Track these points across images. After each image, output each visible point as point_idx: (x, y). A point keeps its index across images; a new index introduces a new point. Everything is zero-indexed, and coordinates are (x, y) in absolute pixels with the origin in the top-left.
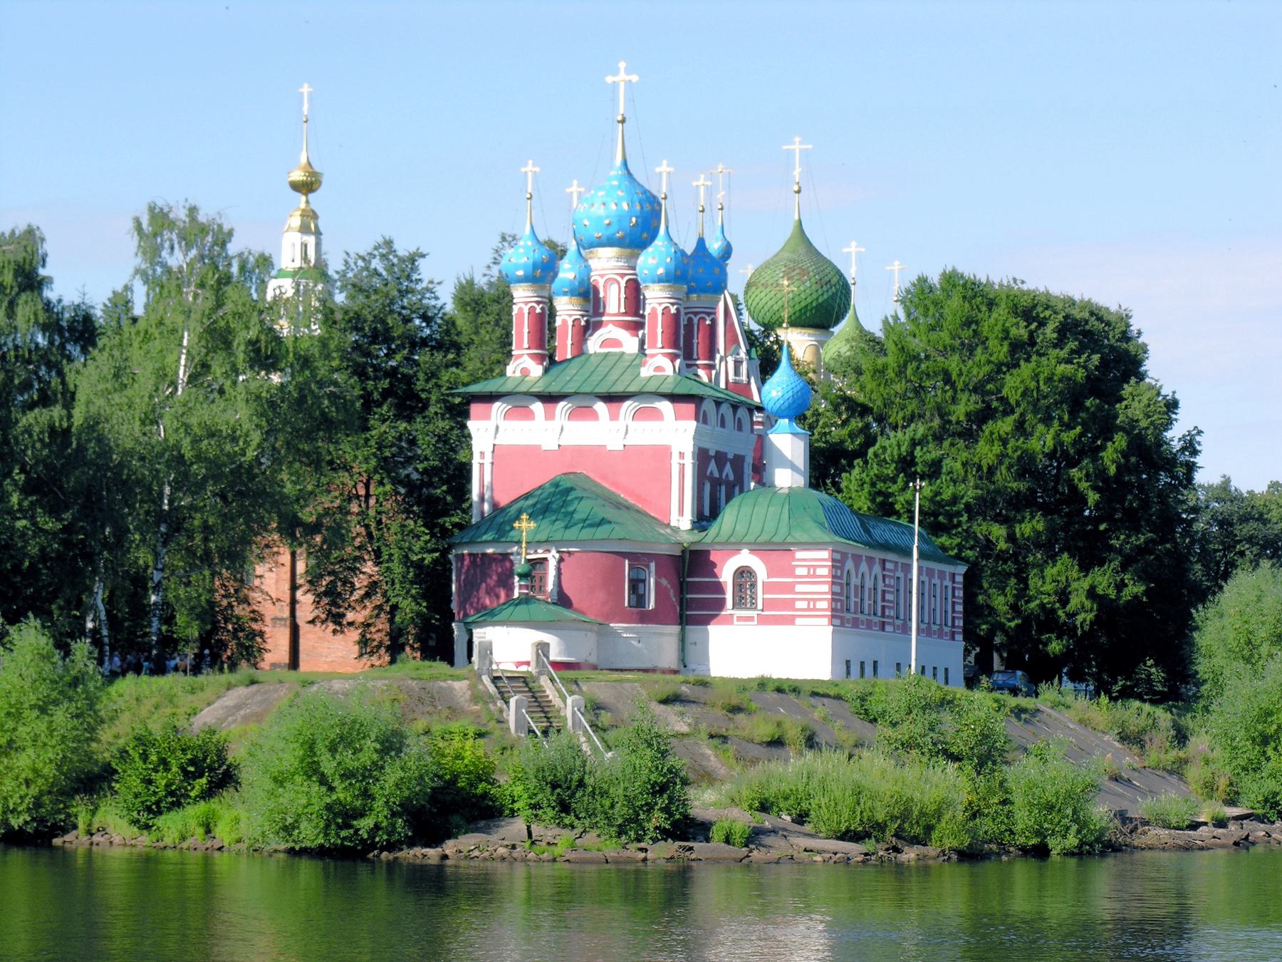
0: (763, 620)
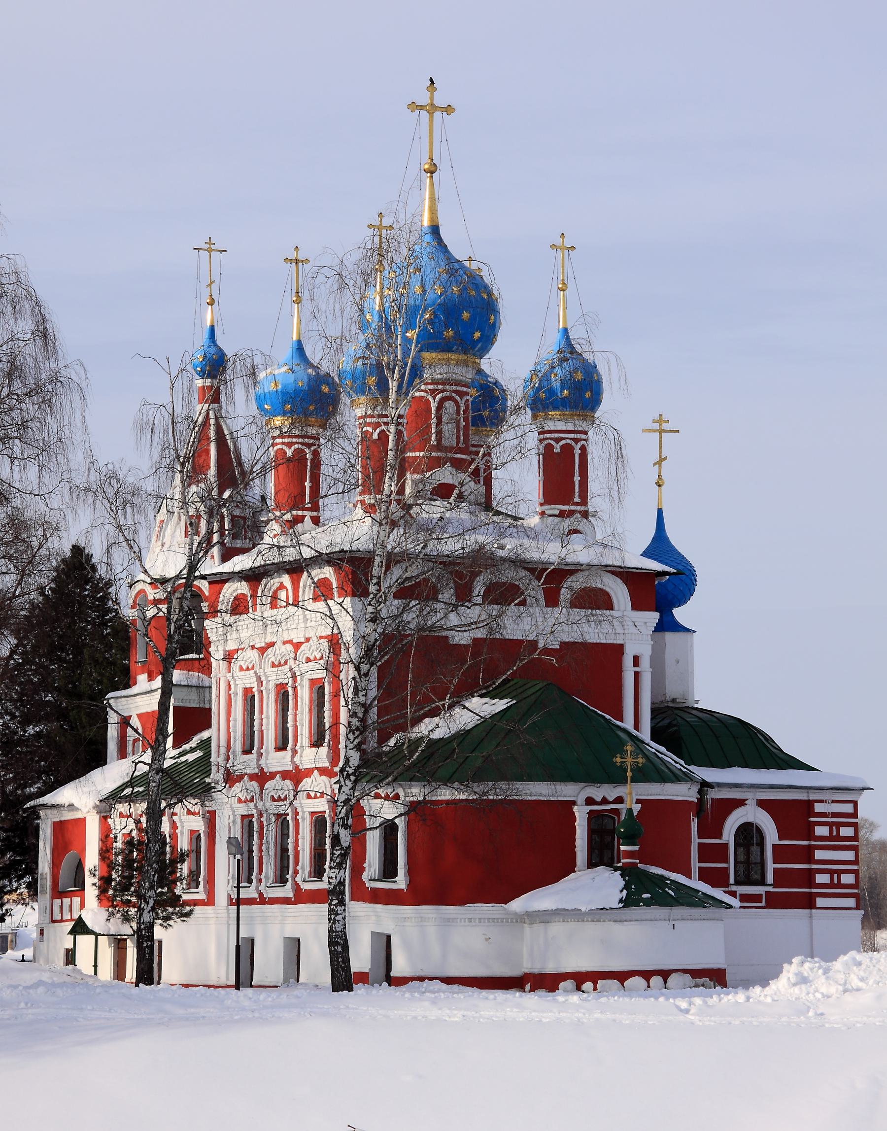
0: (774, 902)
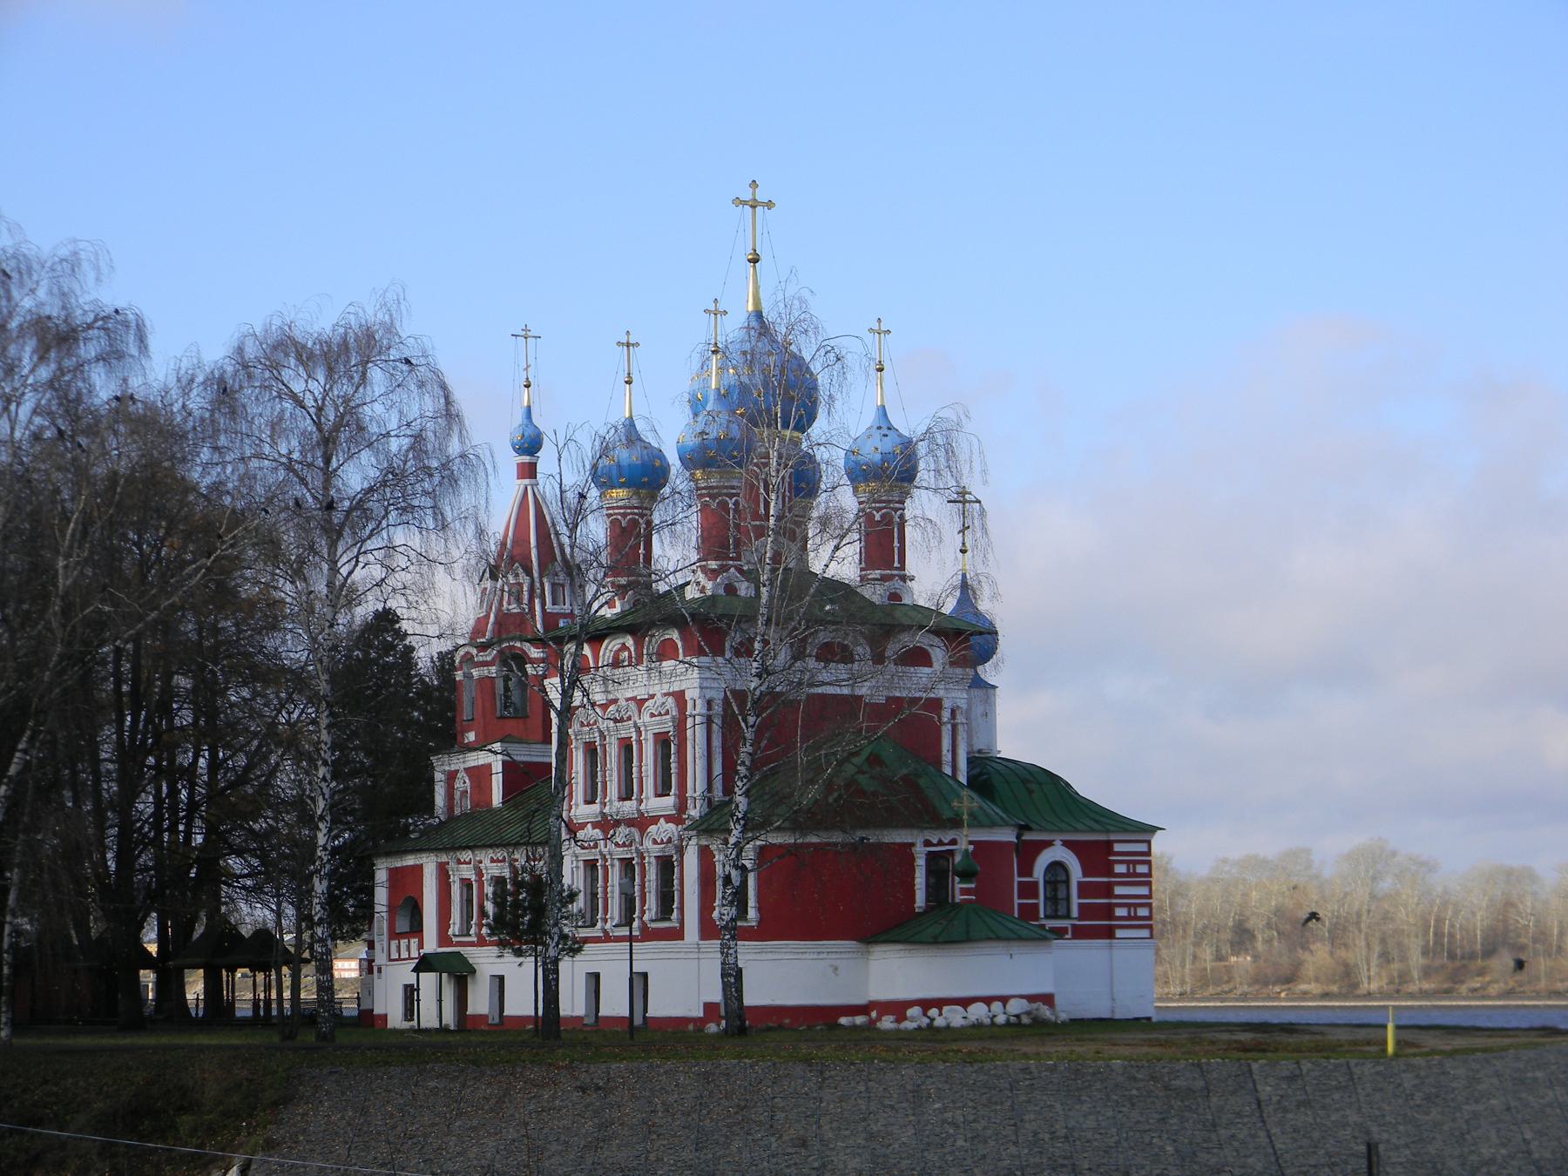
0: (1080, 933)
